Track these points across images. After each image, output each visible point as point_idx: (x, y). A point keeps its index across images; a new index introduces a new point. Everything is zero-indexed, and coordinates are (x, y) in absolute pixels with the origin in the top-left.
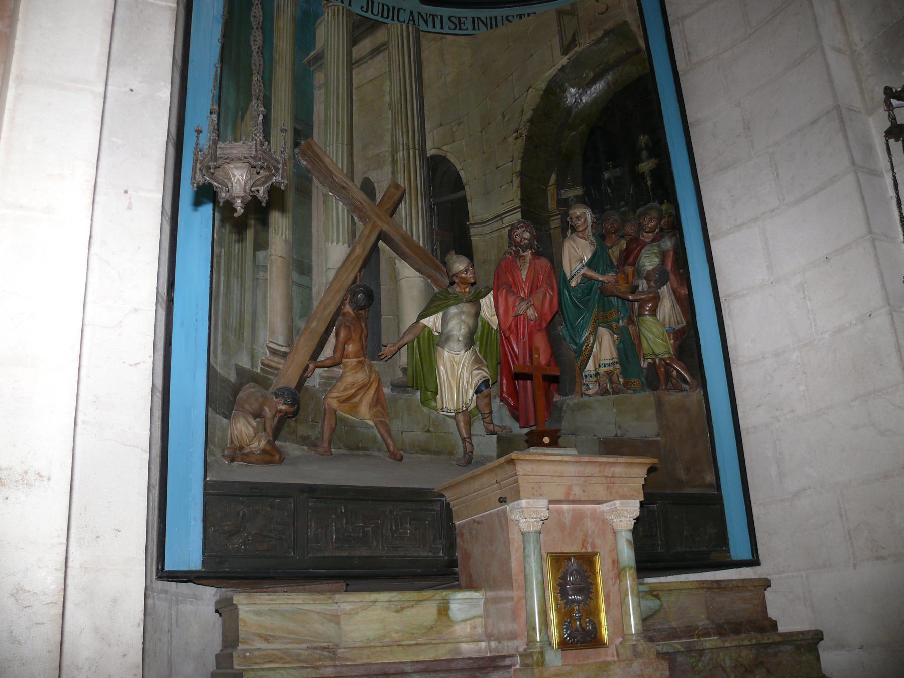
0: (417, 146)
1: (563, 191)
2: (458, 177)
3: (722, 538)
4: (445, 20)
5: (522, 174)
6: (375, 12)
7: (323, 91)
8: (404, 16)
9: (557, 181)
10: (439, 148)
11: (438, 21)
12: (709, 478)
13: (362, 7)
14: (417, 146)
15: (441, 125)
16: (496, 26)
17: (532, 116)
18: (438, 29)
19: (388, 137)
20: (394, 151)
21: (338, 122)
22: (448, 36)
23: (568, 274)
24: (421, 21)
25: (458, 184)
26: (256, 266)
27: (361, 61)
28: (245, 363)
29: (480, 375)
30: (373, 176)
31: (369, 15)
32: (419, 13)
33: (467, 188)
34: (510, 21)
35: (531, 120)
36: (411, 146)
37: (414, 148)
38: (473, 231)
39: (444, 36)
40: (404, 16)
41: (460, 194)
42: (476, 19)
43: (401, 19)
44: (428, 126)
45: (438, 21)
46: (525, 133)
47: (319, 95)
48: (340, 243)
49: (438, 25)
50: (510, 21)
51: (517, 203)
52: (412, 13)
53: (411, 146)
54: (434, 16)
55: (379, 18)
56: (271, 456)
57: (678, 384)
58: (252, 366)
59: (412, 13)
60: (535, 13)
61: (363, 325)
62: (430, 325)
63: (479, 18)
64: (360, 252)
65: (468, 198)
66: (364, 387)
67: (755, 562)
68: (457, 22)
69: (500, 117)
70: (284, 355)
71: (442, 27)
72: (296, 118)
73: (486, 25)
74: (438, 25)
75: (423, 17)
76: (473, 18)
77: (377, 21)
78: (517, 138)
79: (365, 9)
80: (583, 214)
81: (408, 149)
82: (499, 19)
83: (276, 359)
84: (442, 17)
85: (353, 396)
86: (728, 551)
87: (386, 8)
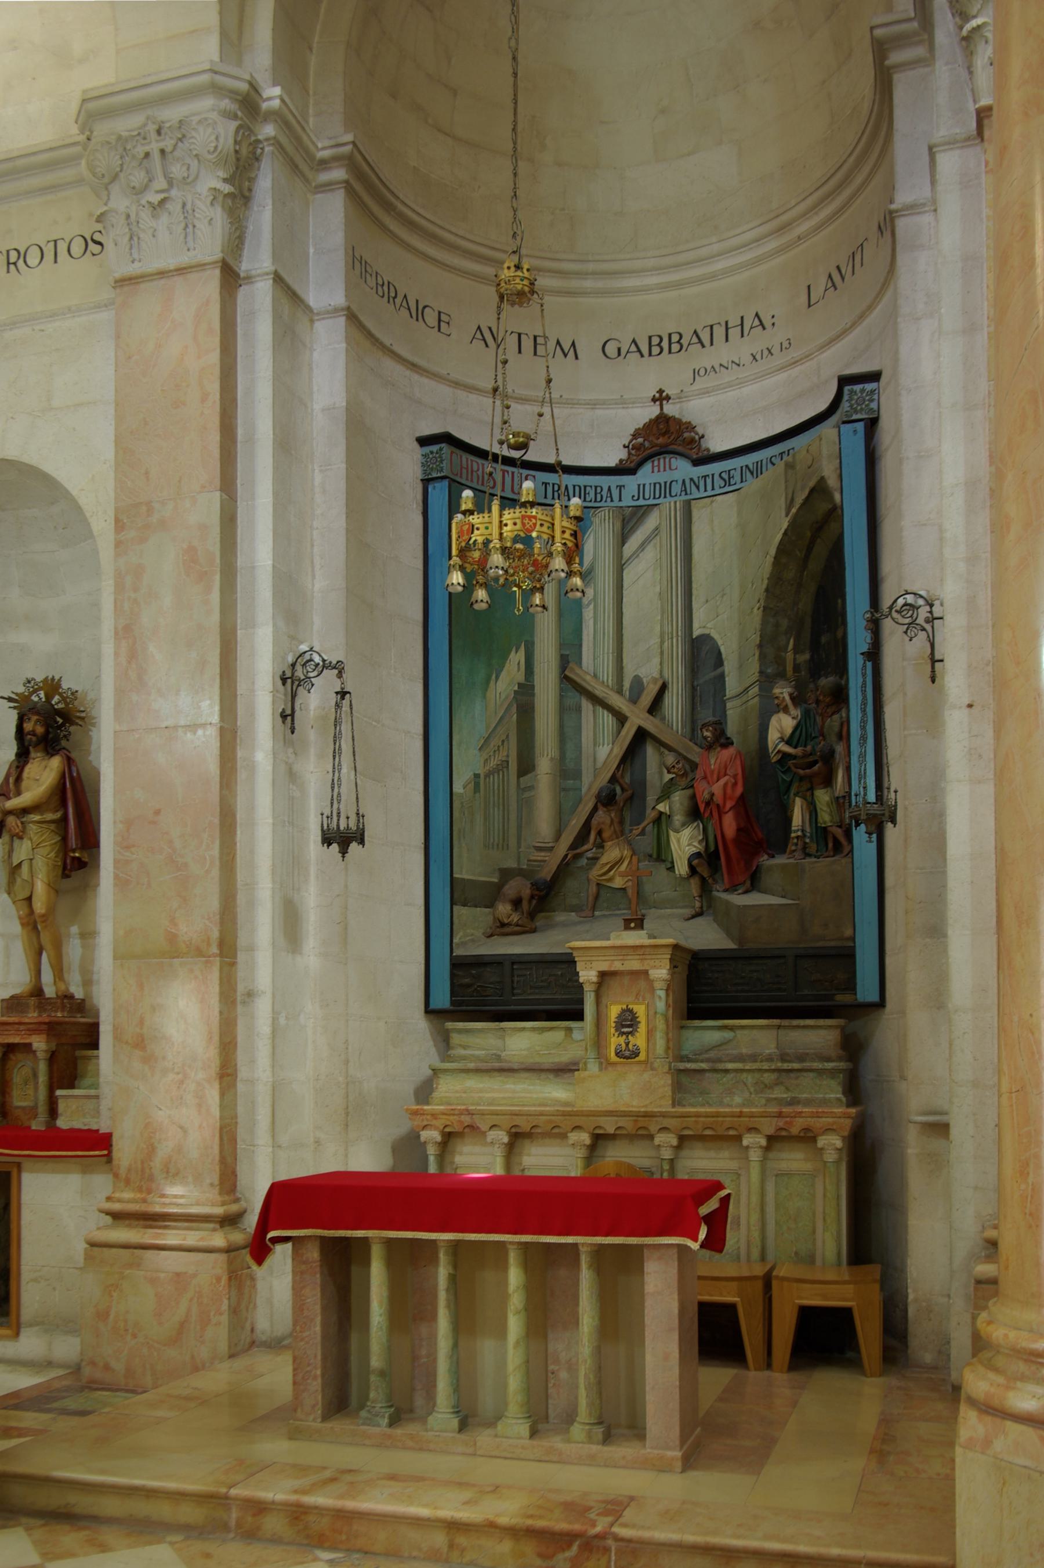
0: (680, 633)
1: (797, 656)
2: (720, 653)
3: (851, 986)
4: (716, 477)
5: (760, 646)
6: (647, 496)
7: (592, 606)
8: (676, 488)
9: (795, 645)
10: (704, 627)
11: (709, 481)
12: (848, 932)
13: (633, 496)
14: (680, 633)
15: (707, 601)
16: (761, 473)
17: (768, 585)
18: (710, 493)
19: (658, 629)
20: (662, 642)
21: (604, 634)
22: (718, 498)
23: (770, 751)
24: (694, 487)
25: (719, 662)
26: (521, 790)
27: (636, 554)
28: (511, 864)
29: (697, 847)
30: (643, 673)
31: (641, 502)
32: (691, 479)
33: (725, 663)
34: (774, 464)
35: (767, 590)
36: (674, 635)
37: (677, 635)
38: (729, 705)
39: (715, 498)
40: (676, 488)
41: (719, 670)
42: (744, 468)
43: (673, 494)
44: (695, 605)
45: (709, 481)
46: (762, 602)
47: (588, 614)
48: (606, 746)
49: (709, 487)
50: (774, 464)
51: (756, 677)
52: (684, 481)
53: (674, 635)
54: (705, 477)
55: (652, 502)
56: (526, 930)
57: (838, 848)
58: (519, 864)
59: (684, 481)
60: (793, 449)
61: (613, 815)
62: (662, 810)
63: (747, 466)
64: (619, 751)
65: (726, 673)
66: (620, 861)
67: (881, 1004)
68: (725, 476)
69: (750, 585)
70: (551, 849)
71: (713, 489)
72: (562, 645)
73: (752, 473)
74: (709, 487)
75: (695, 483)
76: (742, 467)
77: (648, 506)
78: (759, 609)
79: (636, 498)
80: (783, 691)
81: (672, 638)
82: (764, 462)
83: (543, 854)
84: (713, 475)
85: (610, 870)
86: (855, 994)
87: (658, 486)
